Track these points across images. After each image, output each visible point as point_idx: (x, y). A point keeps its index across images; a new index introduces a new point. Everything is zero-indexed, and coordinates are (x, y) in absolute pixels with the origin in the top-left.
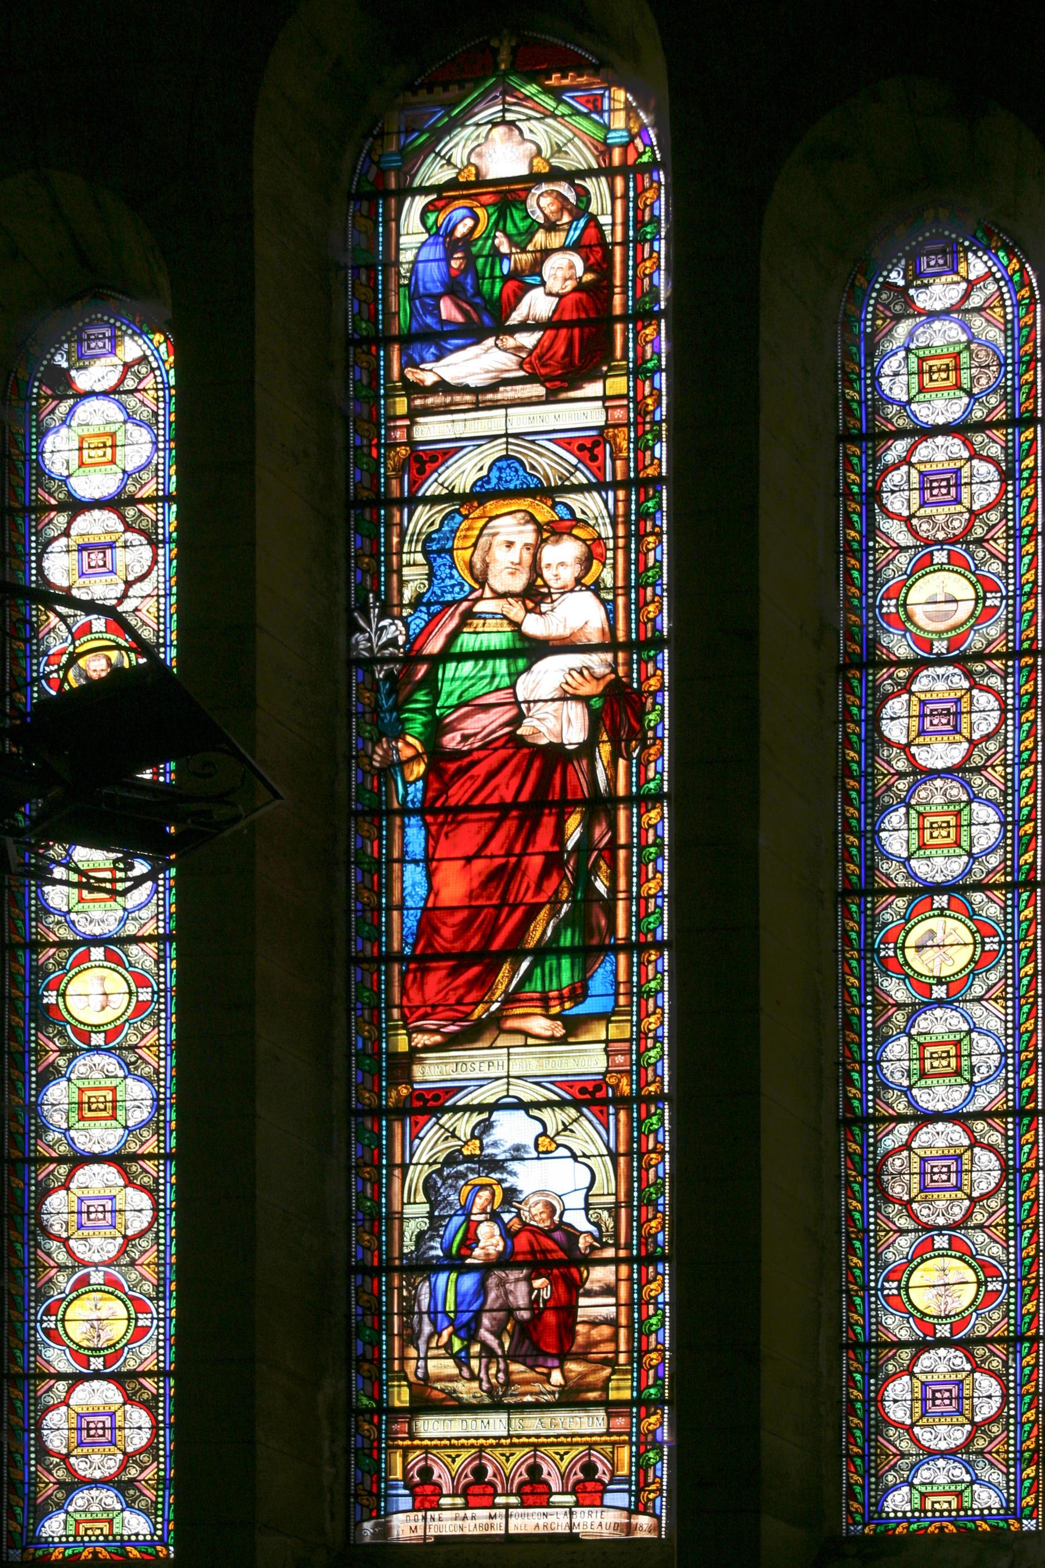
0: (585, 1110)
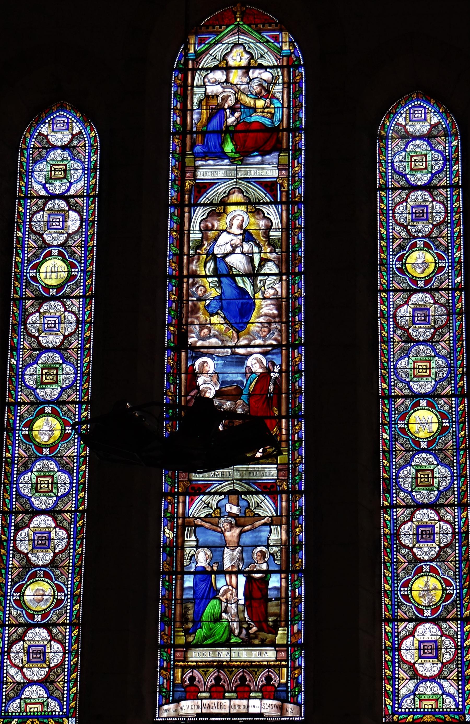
0: (267, 497)
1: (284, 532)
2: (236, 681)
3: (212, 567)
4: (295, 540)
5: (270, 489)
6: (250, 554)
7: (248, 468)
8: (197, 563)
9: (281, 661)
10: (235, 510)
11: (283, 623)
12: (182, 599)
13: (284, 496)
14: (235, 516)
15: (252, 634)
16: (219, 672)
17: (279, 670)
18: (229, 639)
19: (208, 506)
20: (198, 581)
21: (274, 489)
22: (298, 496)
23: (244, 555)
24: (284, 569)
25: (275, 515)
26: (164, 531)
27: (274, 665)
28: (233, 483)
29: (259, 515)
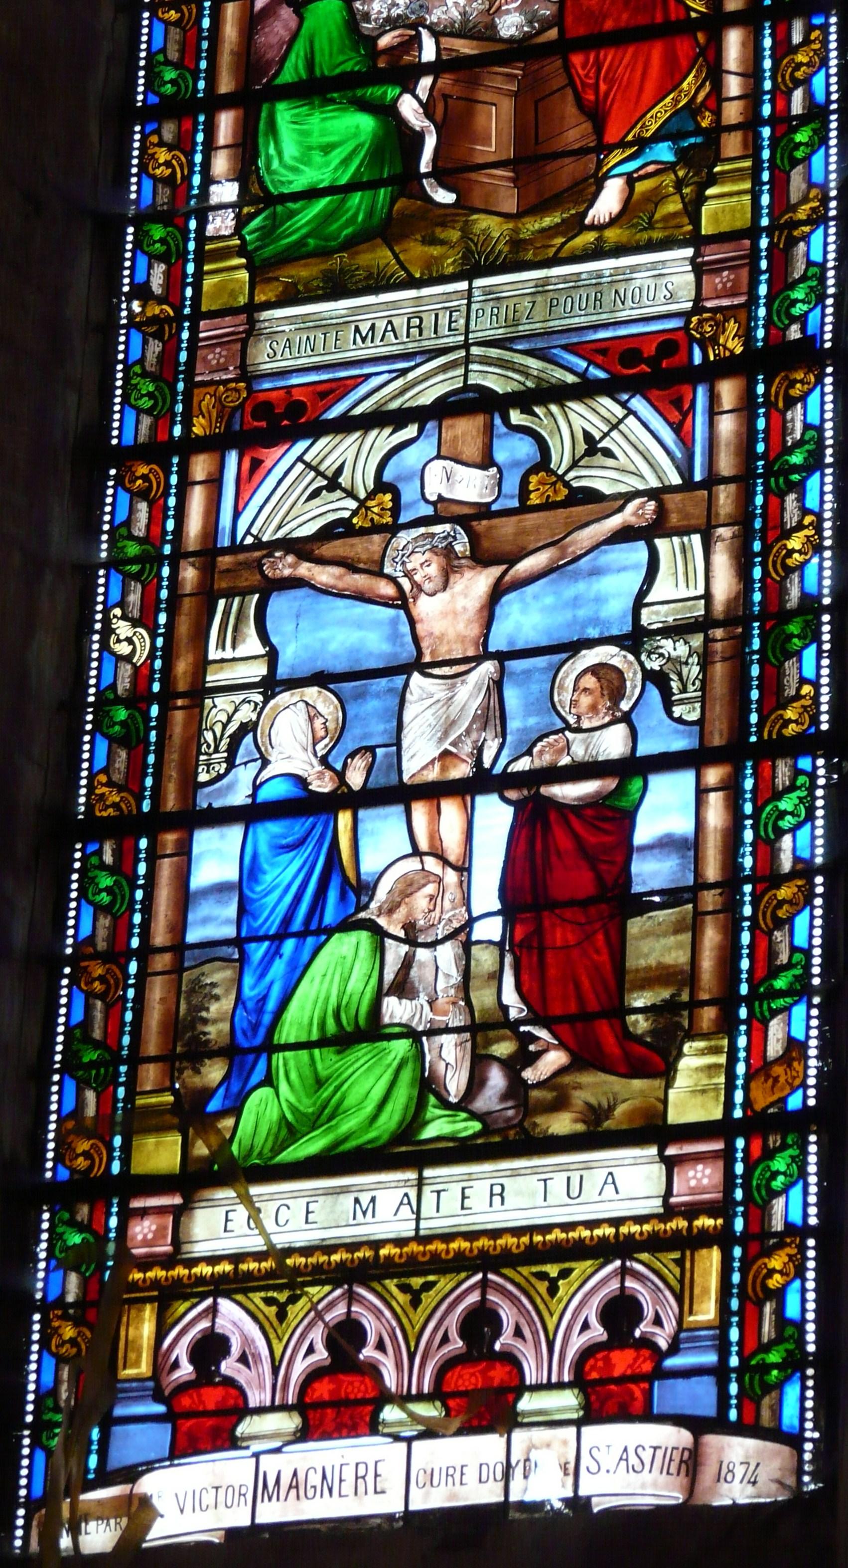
0: (638, 403)
1: (722, 561)
2: (445, 1340)
3: (341, 776)
4: (783, 591)
5: (653, 362)
6: (539, 686)
7: (546, 281)
8: (265, 762)
9: (691, 1211)
10: (471, 486)
11: (709, 1014)
12: (179, 947)
13: (728, 391)
14: (471, 517)
15: (539, 1085)
16: (351, 1298)
17: (680, 1263)
18: (415, 1120)
19: (333, 484)
20: (263, 848)
21: (678, 360)
22: (799, 375)
23: (512, 696)
24: (716, 741)
25: (675, 479)
26: (107, 631)
27: (654, 1235)
28: (468, 360)
29: (592, 496)
